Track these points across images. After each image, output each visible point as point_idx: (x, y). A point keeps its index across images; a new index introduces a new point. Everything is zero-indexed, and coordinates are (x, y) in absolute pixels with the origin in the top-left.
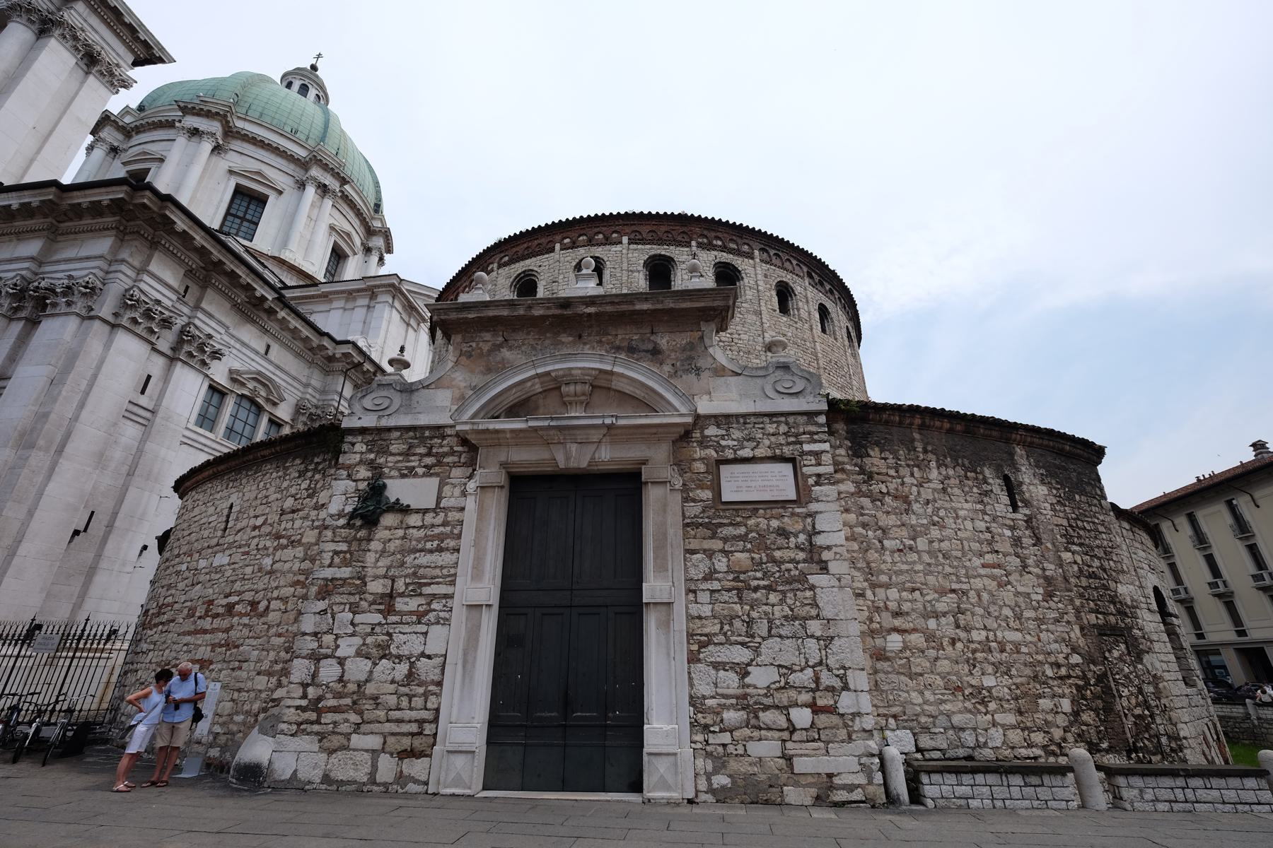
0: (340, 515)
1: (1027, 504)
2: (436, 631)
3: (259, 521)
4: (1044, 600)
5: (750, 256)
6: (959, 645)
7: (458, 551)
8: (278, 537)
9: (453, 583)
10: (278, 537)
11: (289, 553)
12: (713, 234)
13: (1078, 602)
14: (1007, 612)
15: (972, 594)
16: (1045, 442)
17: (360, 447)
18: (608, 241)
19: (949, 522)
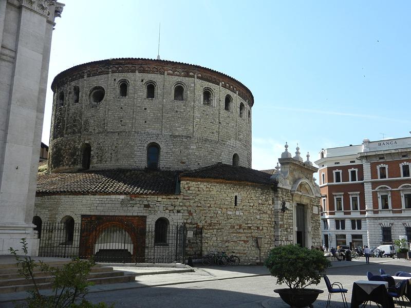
0: (280, 209)
2: (292, 235)
3: (252, 205)
7: (292, 219)
8: (259, 210)
9: (293, 226)
10: (259, 210)
11: (264, 215)
17: (280, 193)
18: (233, 91)
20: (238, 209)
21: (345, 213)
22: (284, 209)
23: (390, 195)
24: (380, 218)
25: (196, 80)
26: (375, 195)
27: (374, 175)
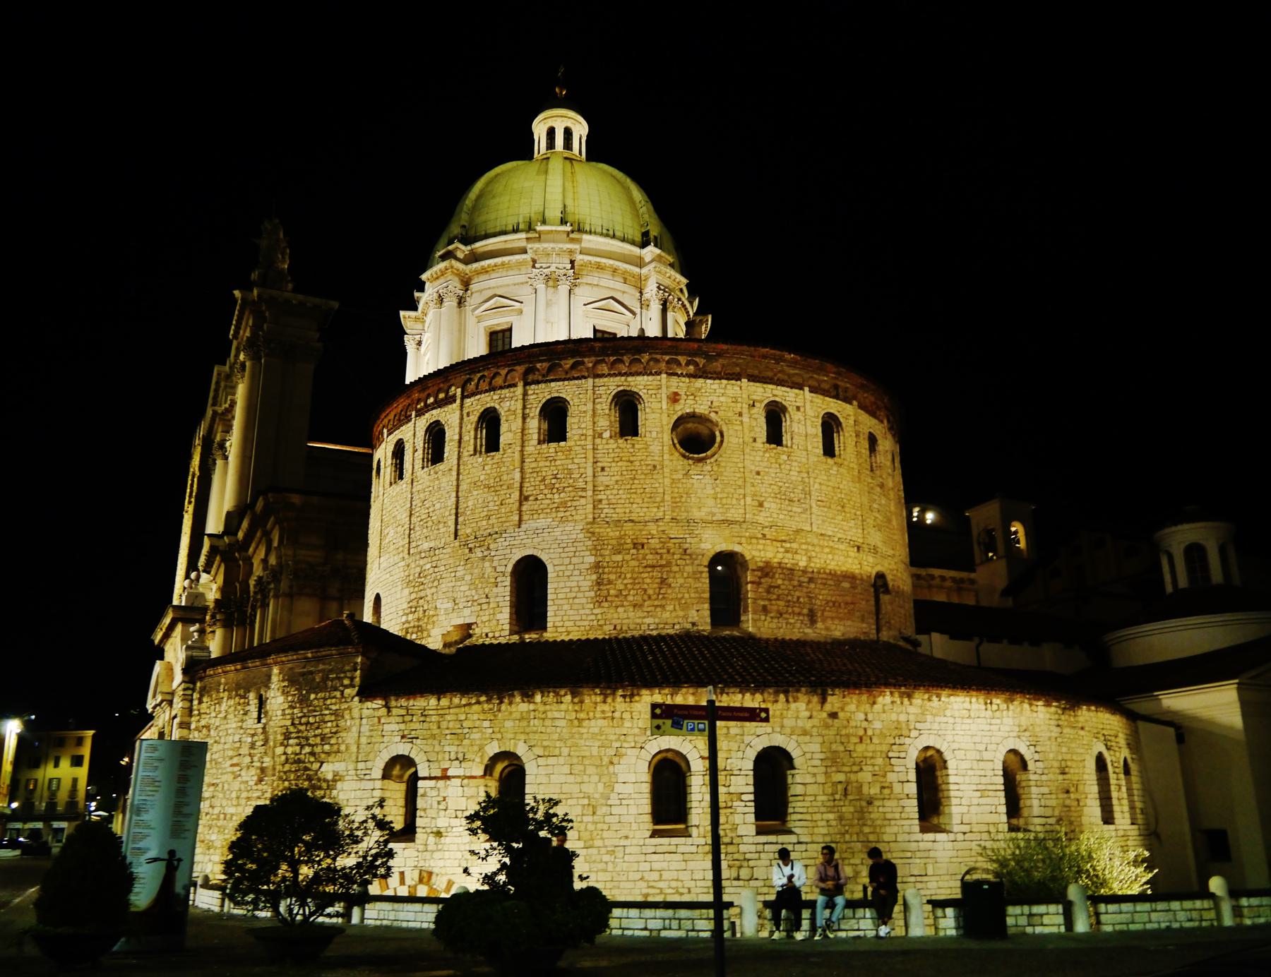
1: (266, 713)
4: (256, 784)
5: (451, 400)
6: (208, 816)
12: (426, 393)
13: (275, 784)
14: (234, 795)
15: (220, 785)
16: (290, 658)
19: (223, 740)
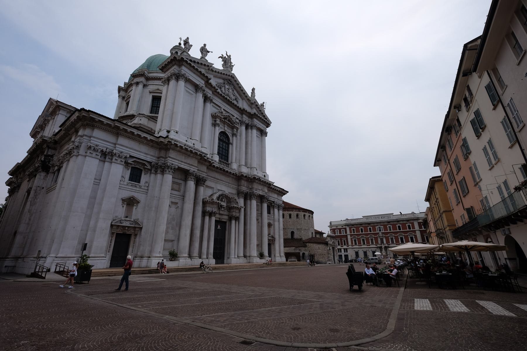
20: (319, 250)
21: (341, 246)
22: (330, 249)
23: (357, 239)
24: (354, 248)
25: (302, 212)
26: (351, 239)
27: (351, 232)
